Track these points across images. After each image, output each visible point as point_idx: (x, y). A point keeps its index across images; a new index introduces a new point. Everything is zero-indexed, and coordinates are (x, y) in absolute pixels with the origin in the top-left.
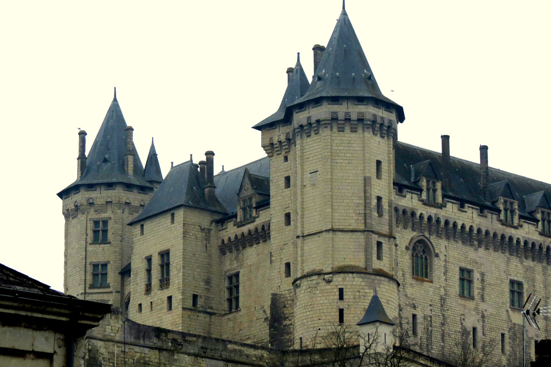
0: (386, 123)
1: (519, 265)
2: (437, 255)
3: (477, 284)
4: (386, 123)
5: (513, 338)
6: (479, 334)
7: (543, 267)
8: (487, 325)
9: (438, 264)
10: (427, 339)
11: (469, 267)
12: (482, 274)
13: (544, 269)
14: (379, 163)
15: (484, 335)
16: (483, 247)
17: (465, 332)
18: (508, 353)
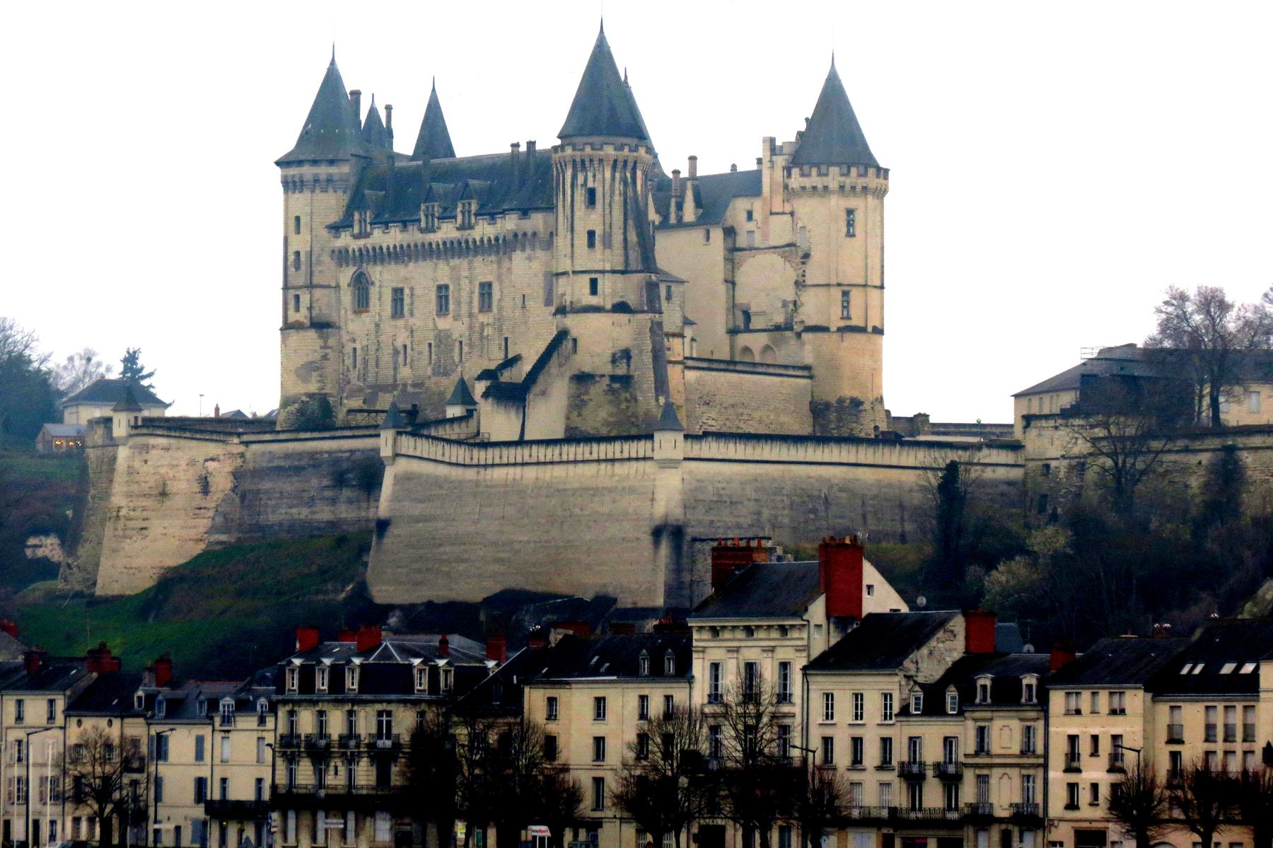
0: (297, 179)
1: (446, 267)
2: (373, 283)
3: (407, 300)
4: (297, 179)
5: (438, 346)
6: (409, 350)
7: (469, 261)
8: (416, 339)
9: (374, 292)
10: (364, 368)
11: (400, 286)
12: (412, 289)
13: (470, 263)
14: (298, 219)
15: (412, 350)
16: (413, 260)
17: (396, 352)
18: (433, 362)
